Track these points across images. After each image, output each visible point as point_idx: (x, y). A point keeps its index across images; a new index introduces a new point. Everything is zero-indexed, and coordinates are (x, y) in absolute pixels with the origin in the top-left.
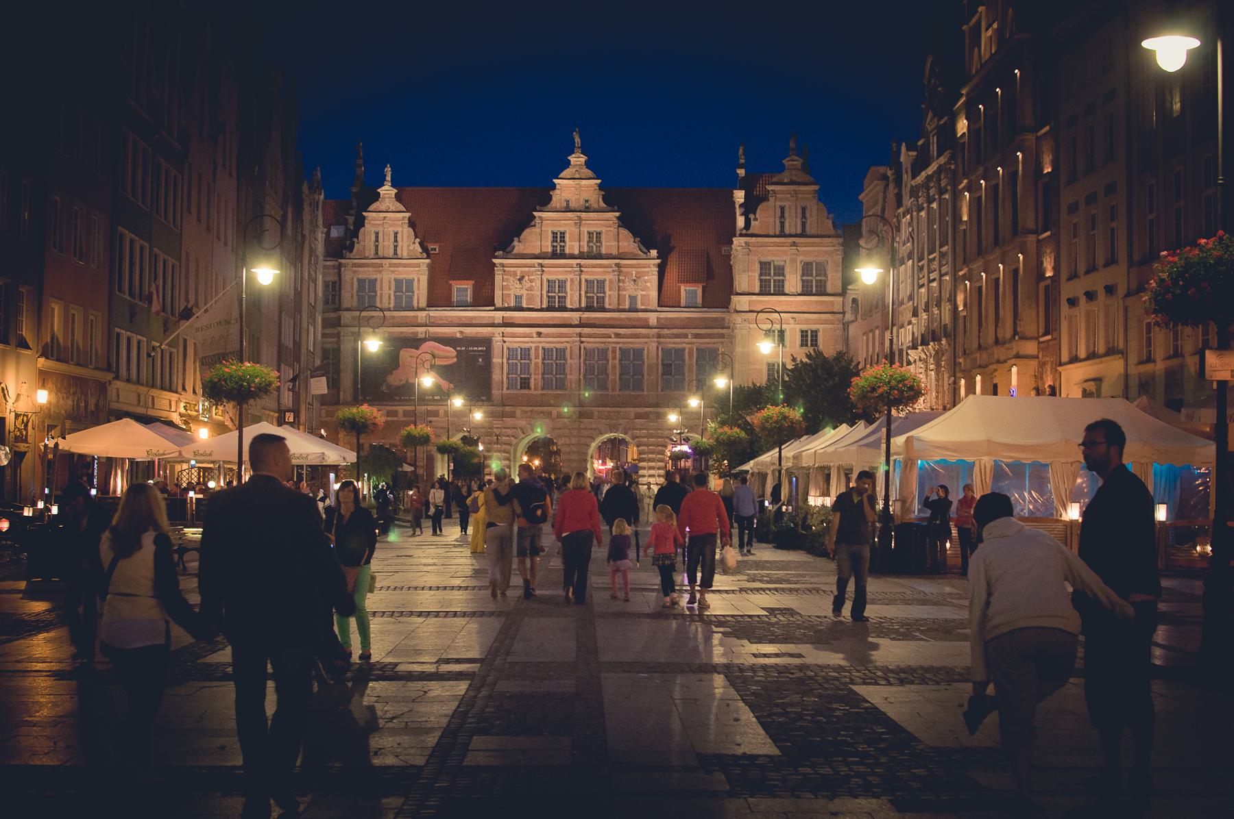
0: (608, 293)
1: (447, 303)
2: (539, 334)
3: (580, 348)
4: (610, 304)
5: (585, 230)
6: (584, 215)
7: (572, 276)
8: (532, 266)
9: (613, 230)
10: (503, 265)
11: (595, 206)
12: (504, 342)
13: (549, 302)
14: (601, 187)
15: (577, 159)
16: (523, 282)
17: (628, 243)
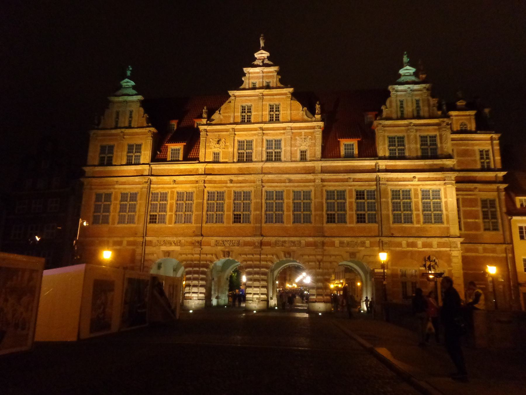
0: (283, 149)
1: (164, 160)
2: (231, 181)
3: (262, 190)
4: (285, 157)
5: (267, 104)
6: (266, 92)
7: (257, 137)
8: (227, 130)
9: (289, 101)
10: (206, 131)
11: (275, 85)
12: (205, 187)
13: (239, 157)
14: (279, 73)
15: (262, 55)
16: (221, 142)
17: (299, 110)
